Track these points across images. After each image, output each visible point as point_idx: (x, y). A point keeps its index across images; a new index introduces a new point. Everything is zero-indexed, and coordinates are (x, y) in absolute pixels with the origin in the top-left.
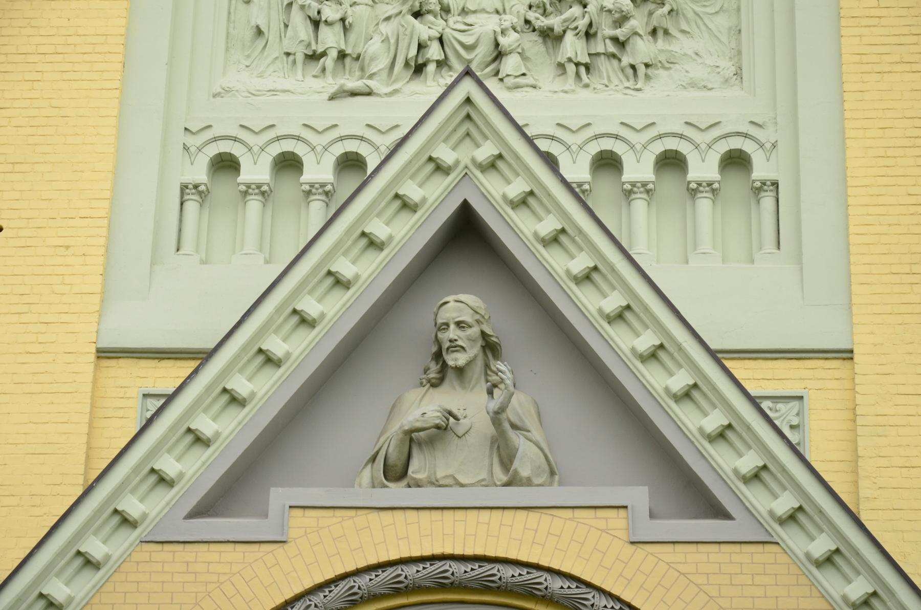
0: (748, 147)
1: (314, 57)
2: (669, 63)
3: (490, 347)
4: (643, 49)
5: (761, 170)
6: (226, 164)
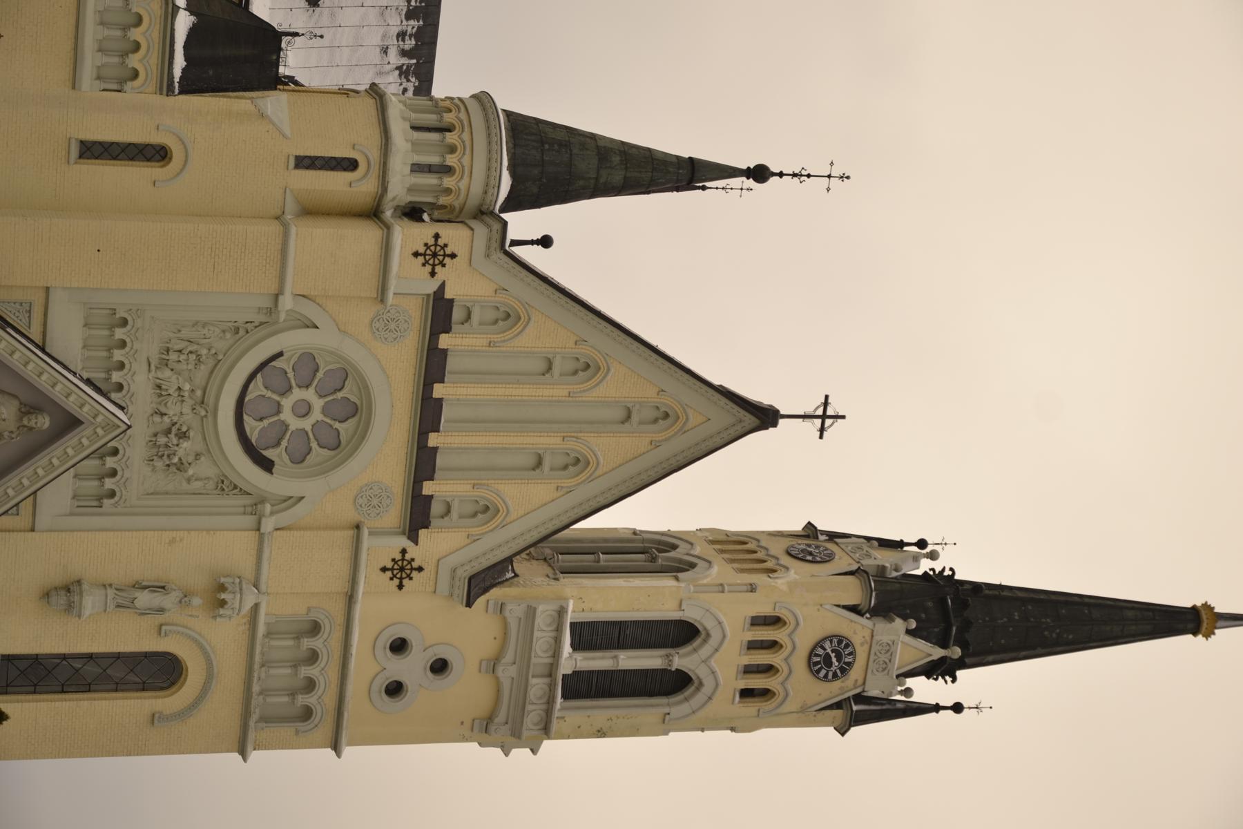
0: (116, 499)
1: (168, 350)
2: (154, 469)
3: (31, 429)
4: (159, 464)
5: (106, 502)
6: (124, 322)
